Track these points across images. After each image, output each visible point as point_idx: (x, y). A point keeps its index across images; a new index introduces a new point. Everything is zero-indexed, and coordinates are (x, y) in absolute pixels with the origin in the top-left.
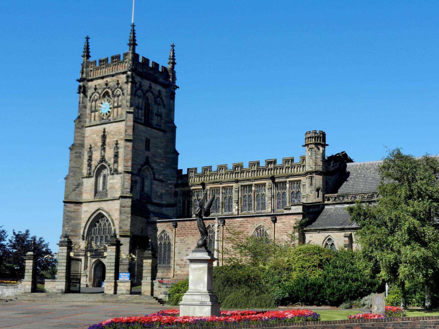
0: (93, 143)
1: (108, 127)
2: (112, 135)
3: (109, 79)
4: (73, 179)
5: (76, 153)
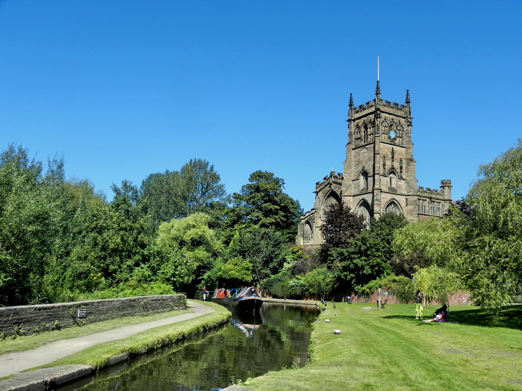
1: (396, 148)
3: (394, 117)
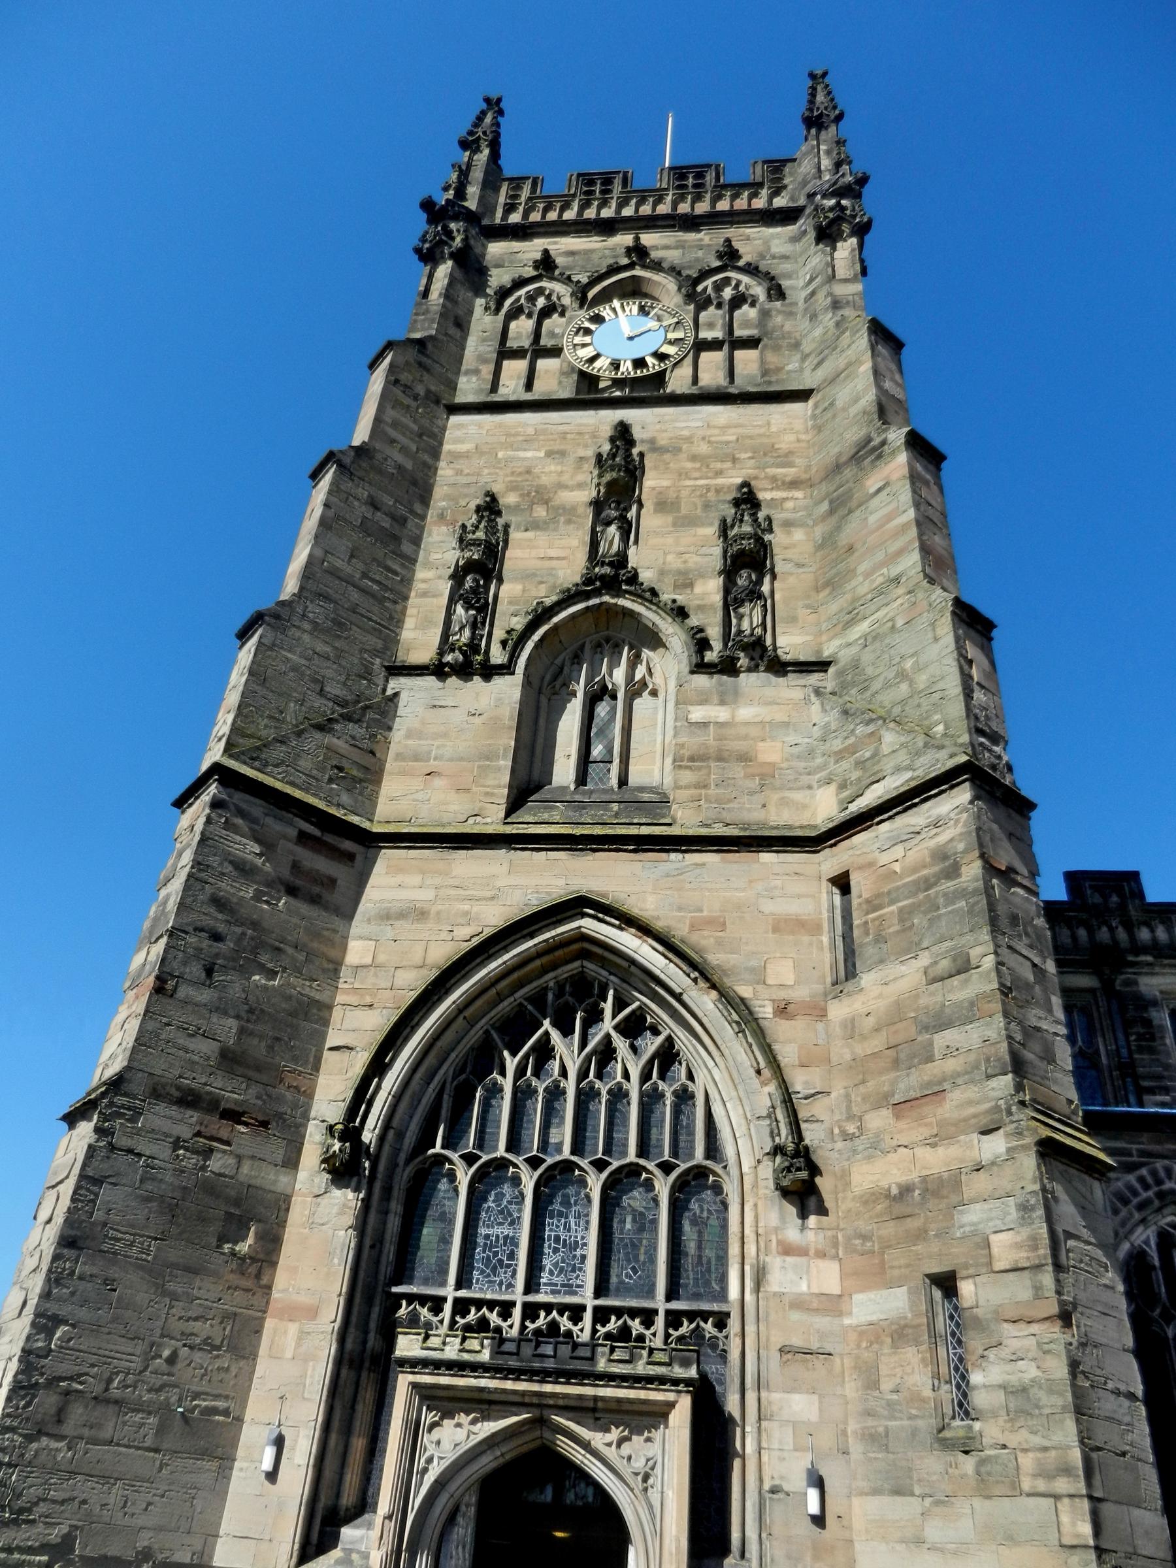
0: (513, 487)
2: (694, 458)
4: (321, 647)
5: (374, 504)
